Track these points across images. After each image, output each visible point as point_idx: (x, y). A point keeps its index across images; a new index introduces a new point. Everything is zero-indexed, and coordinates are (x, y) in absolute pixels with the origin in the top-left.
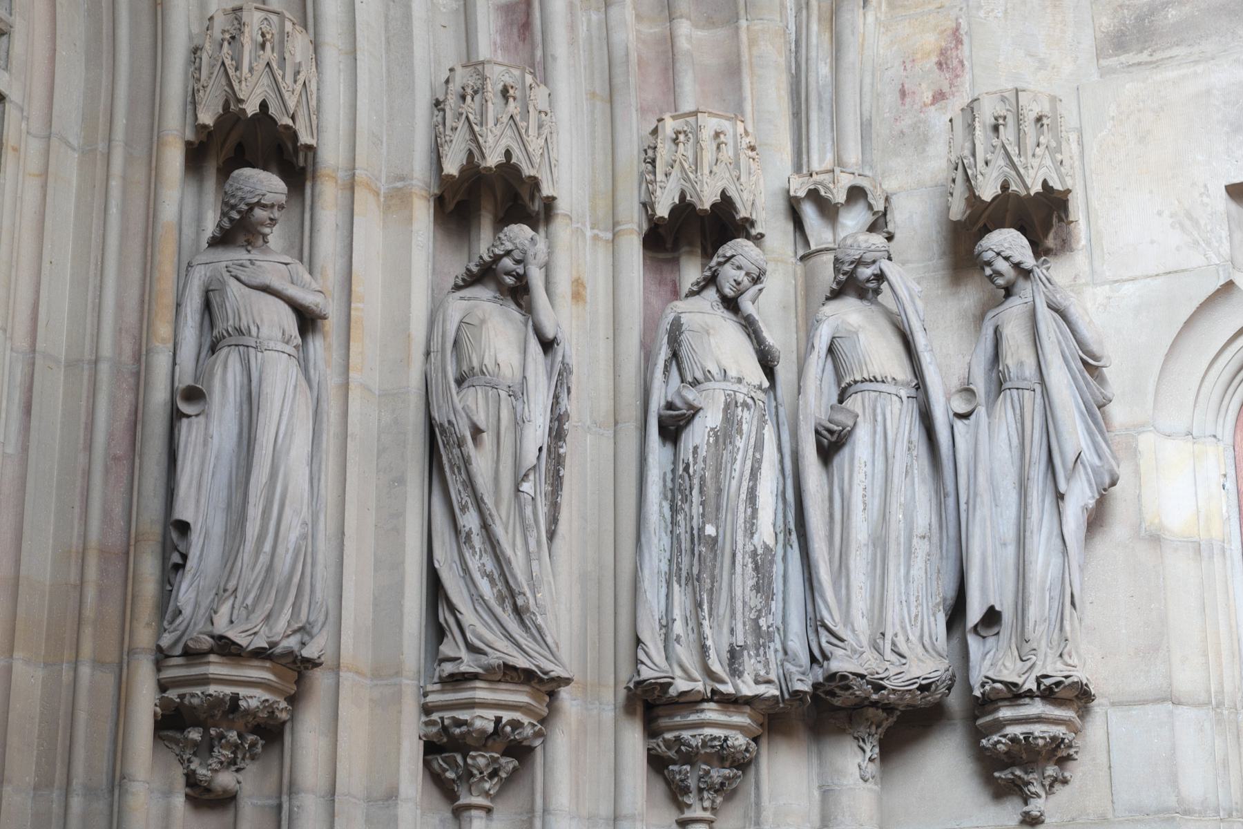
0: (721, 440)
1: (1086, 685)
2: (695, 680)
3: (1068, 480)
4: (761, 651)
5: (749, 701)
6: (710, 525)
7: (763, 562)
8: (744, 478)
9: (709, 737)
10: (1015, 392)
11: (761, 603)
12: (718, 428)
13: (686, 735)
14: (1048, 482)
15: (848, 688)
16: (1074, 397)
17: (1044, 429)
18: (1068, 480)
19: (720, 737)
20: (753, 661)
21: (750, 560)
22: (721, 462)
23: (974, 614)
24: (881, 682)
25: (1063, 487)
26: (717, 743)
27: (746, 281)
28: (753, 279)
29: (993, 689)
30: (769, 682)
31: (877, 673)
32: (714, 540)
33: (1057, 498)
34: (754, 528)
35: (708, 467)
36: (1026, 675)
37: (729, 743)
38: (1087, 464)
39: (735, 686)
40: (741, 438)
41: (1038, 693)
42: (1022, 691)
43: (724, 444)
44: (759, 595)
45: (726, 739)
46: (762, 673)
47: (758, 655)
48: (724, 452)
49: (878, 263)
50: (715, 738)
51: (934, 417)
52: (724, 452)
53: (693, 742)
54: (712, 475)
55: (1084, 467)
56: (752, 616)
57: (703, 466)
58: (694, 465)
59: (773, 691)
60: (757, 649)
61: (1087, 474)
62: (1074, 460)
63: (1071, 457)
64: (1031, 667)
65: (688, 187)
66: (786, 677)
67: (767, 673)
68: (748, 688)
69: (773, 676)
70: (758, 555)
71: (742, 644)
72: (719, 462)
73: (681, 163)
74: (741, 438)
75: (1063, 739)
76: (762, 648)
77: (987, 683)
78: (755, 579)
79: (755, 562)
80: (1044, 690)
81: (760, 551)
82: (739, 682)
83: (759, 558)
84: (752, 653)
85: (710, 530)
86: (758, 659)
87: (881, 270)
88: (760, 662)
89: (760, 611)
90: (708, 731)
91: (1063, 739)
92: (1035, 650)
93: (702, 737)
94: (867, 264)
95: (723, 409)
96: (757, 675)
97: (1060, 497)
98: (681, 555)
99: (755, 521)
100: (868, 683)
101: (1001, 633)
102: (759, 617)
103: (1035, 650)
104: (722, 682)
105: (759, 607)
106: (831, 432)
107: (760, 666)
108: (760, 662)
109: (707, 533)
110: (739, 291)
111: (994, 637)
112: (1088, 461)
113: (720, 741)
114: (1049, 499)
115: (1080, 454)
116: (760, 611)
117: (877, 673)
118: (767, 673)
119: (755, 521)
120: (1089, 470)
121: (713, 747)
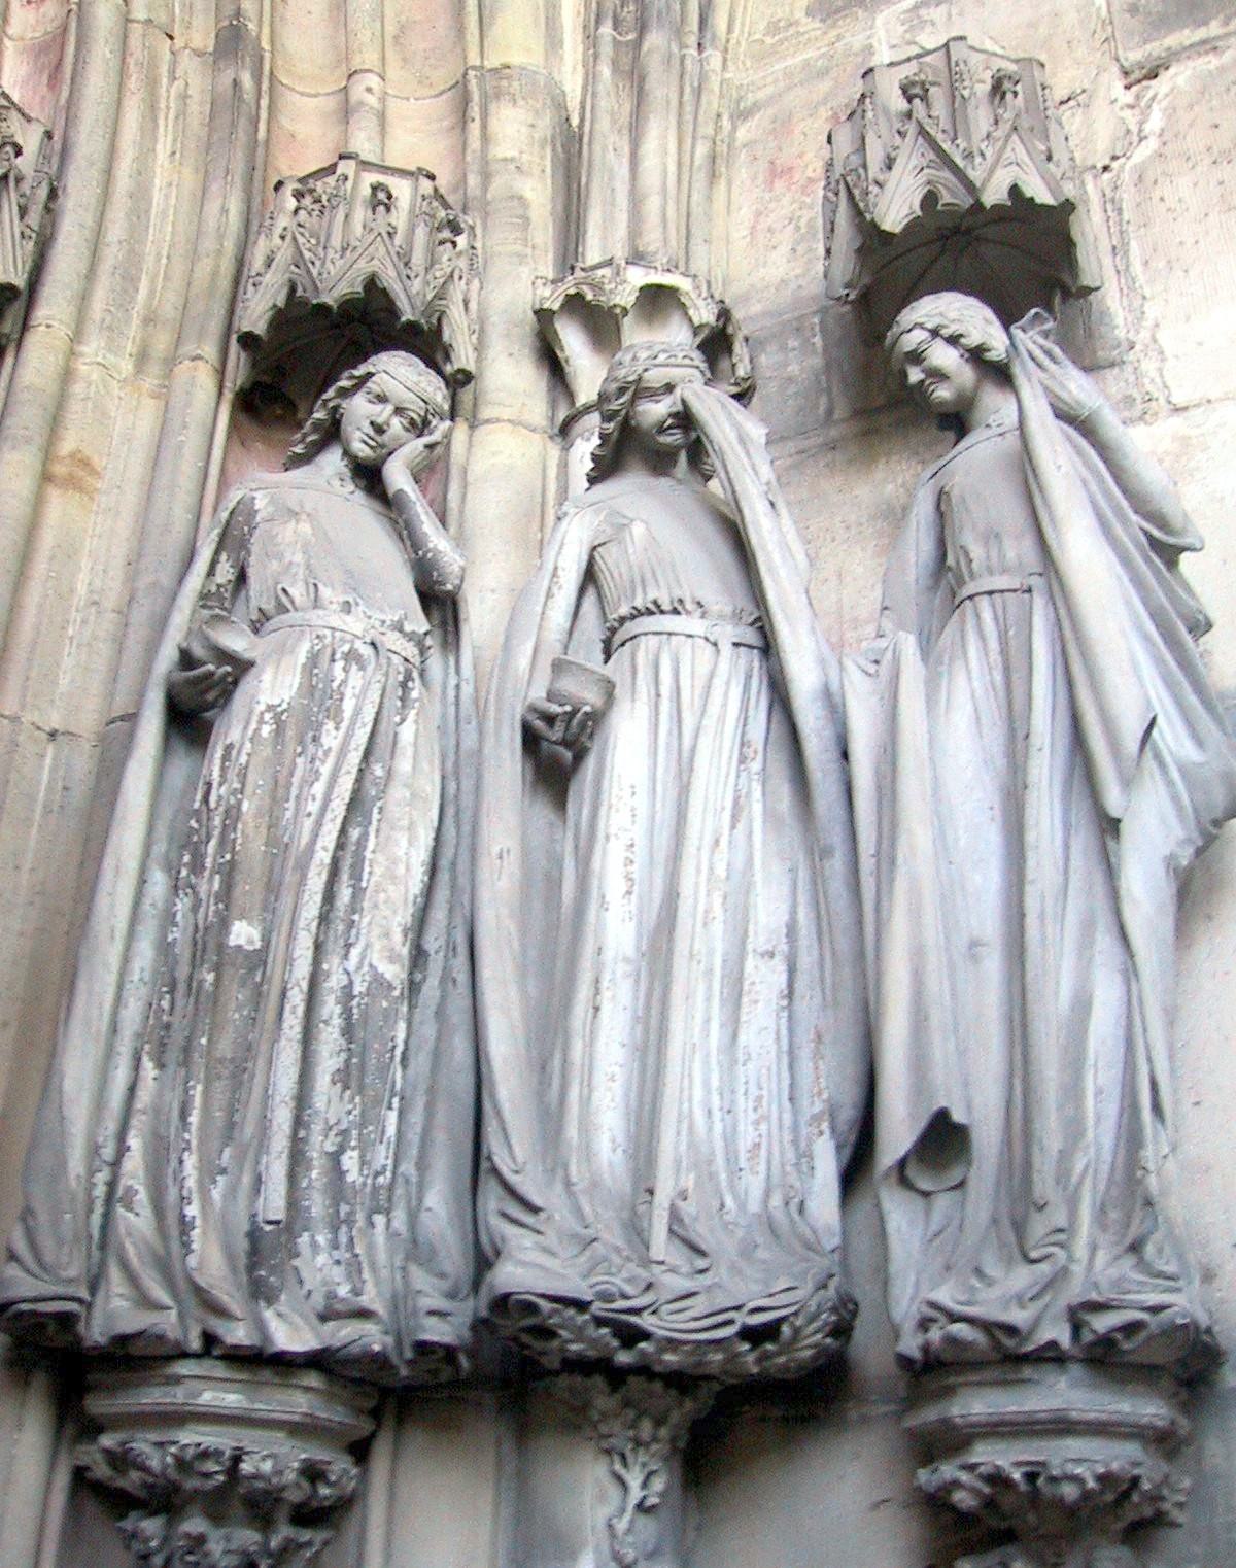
0: (290, 733)
1: (1209, 1331)
2: (162, 1308)
3: (1127, 782)
4: (343, 1239)
5: (318, 1361)
6: (244, 923)
7: (365, 1015)
8: (329, 815)
9: (191, 1451)
10: (984, 602)
11: (350, 1112)
12: (285, 706)
13: (143, 1445)
14: (1075, 797)
15: (547, 1333)
16: (1128, 602)
17: (1060, 670)
18: (1127, 782)
19: (218, 1453)
20: (322, 1259)
21: (338, 1009)
22: (289, 785)
23: (897, 1134)
24: (633, 1319)
25: (1114, 801)
26: (211, 1466)
27: (397, 425)
28: (412, 422)
29: (951, 1341)
30: (364, 1314)
31: (625, 1297)
32: (258, 960)
33: (1103, 832)
34: (354, 932)
35: (249, 789)
36: (1039, 1304)
37: (246, 1467)
38: (1168, 759)
39: (261, 1326)
40: (337, 729)
41: (1076, 1351)
42: (1029, 1347)
43: (301, 742)
44: (348, 1092)
45: (237, 1459)
46: (343, 1291)
47: (335, 1245)
48: (300, 761)
49: (678, 392)
50: (205, 1455)
51: (788, 677)
52: (300, 761)
53: (154, 1463)
54: (259, 808)
55: (1162, 765)
56: (330, 1148)
57: (237, 785)
58: (221, 785)
59: (372, 1337)
60: (335, 1230)
61: (1170, 783)
62: (1140, 734)
63: (1131, 731)
64: (1051, 1284)
65: (302, 282)
66: (401, 1301)
67: (357, 1292)
68: (290, 1334)
69: (370, 1298)
70: (353, 998)
71: (280, 1215)
72: (282, 781)
73: (294, 239)
74: (337, 729)
75: (1135, 1482)
76: (344, 1229)
77: (933, 1320)
78: (344, 1056)
79: (347, 1013)
80: (1093, 1344)
81: (359, 988)
82: (268, 1314)
83: (355, 1003)
84: (321, 1239)
85: (243, 934)
86: (336, 1254)
87: (684, 402)
88: (338, 1262)
89: (344, 1133)
90: (190, 1437)
91: (1135, 1482)
92: (1061, 1231)
93: (173, 1449)
94: (653, 394)
95: (304, 665)
96: (331, 1296)
97: (1109, 827)
98: (172, 992)
99: (356, 917)
100: (600, 1322)
101: (972, 1183)
102: (341, 1149)
103: (1061, 1231)
104: (222, 1312)
105: (344, 1126)
106: (550, 719)
107: (337, 1273)
108: (338, 1262)
109: (233, 941)
110: (382, 446)
111: (952, 1193)
112: (1171, 753)
113: (218, 1462)
114: (1083, 840)
115: (1153, 723)
116: (344, 1133)
117: (625, 1297)
118: (357, 1292)
119: (356, 917)
120: (1175, 774)
121: (207, 1476)
